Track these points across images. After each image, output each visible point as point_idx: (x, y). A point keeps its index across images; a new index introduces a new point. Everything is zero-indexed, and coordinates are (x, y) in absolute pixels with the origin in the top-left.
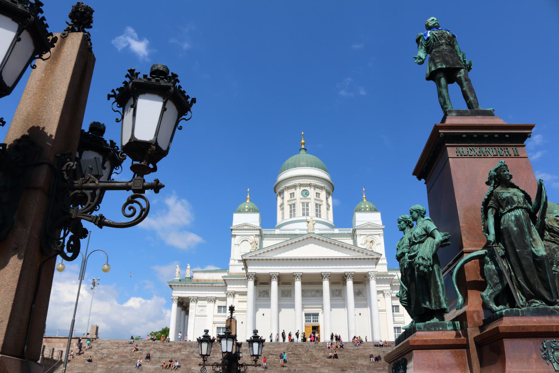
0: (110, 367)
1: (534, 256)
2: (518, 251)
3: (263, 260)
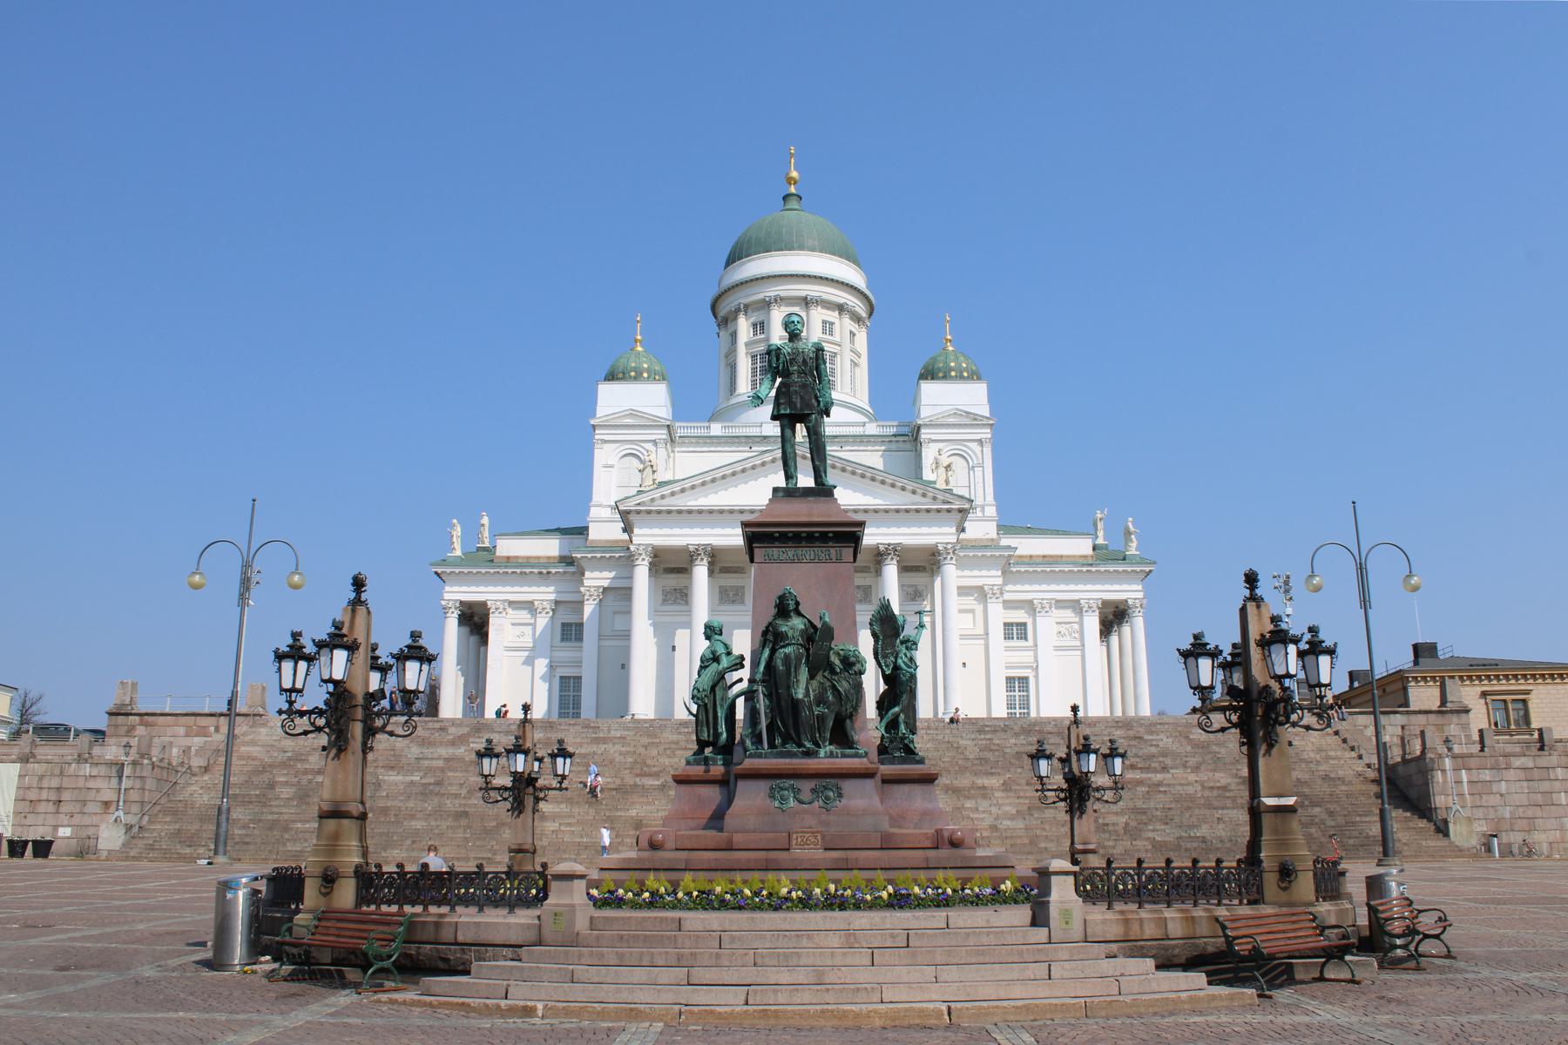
0: (304, 782)
3: (669, 512)
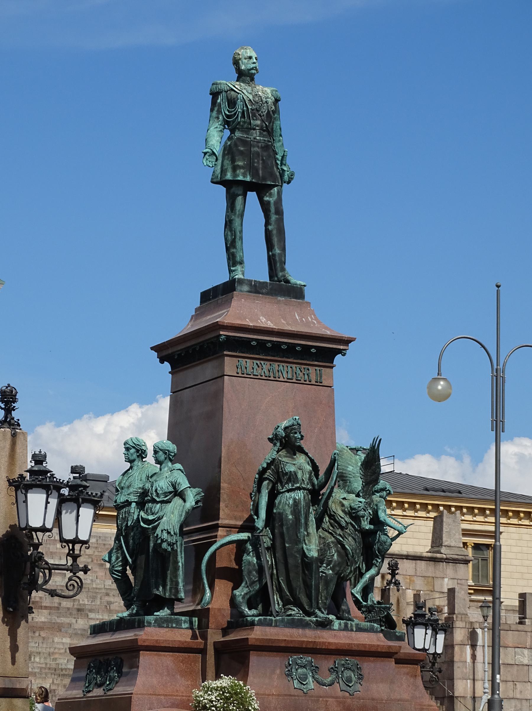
1: (304, 555)
2: (287, 545)
